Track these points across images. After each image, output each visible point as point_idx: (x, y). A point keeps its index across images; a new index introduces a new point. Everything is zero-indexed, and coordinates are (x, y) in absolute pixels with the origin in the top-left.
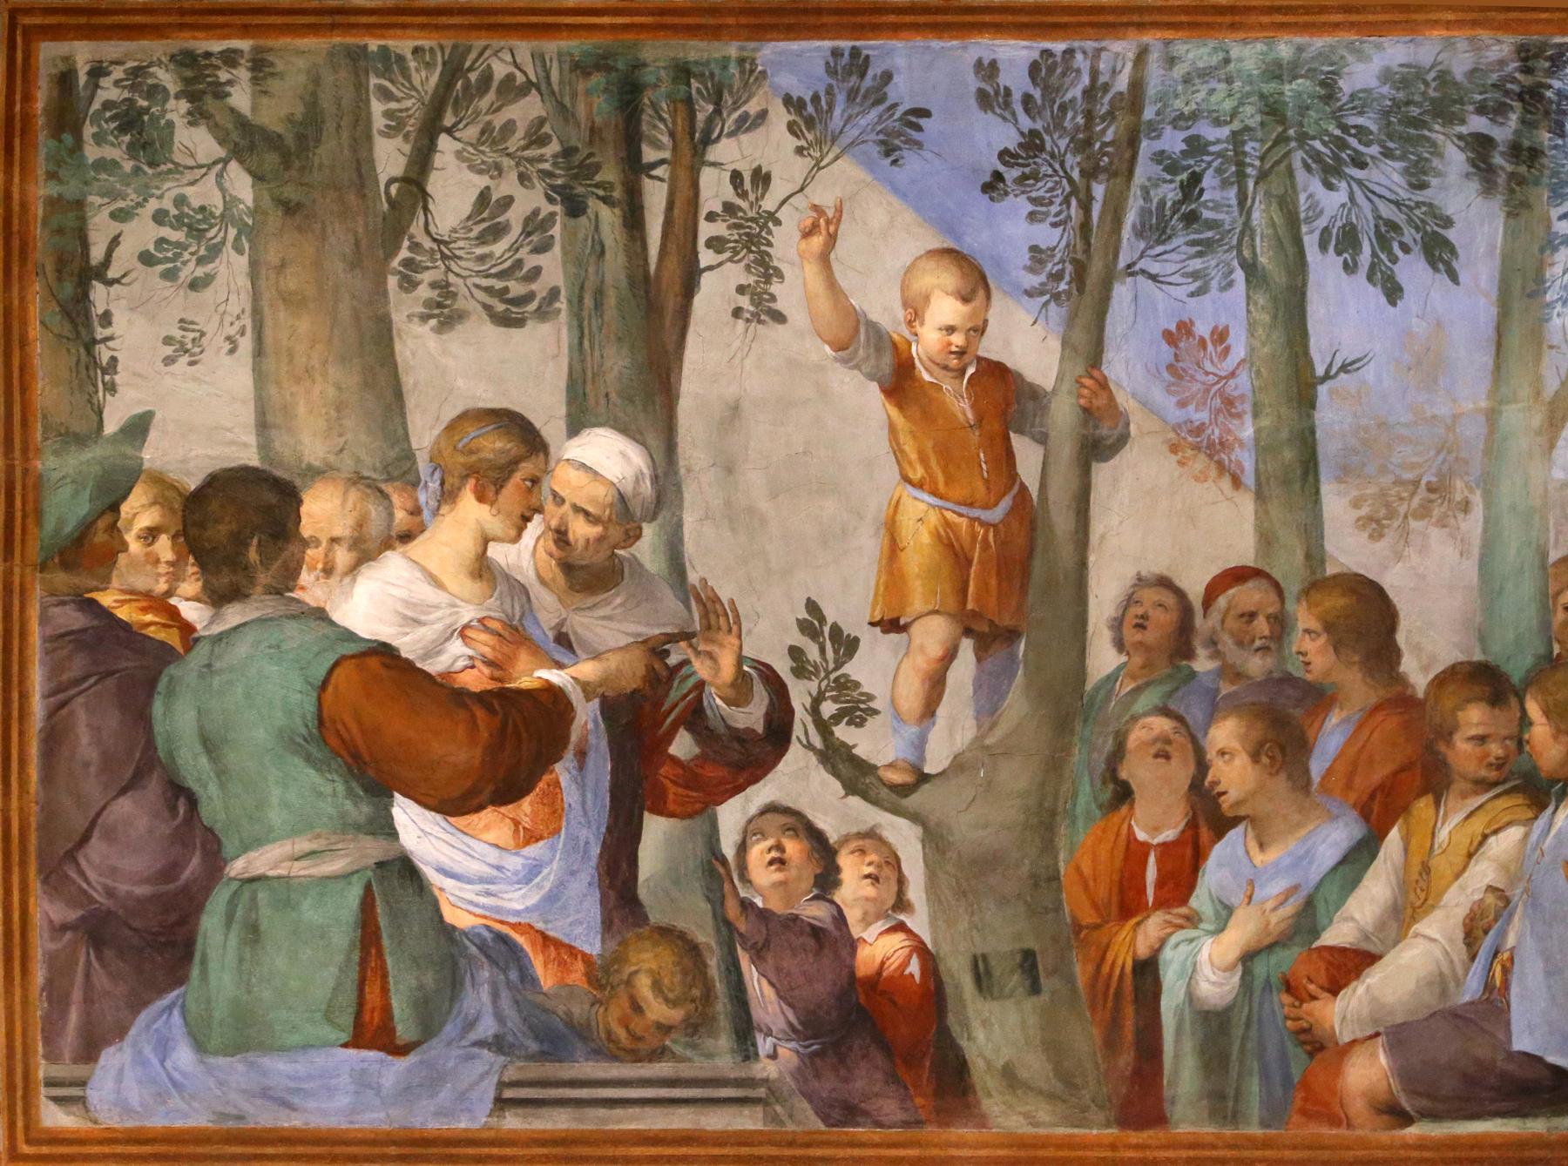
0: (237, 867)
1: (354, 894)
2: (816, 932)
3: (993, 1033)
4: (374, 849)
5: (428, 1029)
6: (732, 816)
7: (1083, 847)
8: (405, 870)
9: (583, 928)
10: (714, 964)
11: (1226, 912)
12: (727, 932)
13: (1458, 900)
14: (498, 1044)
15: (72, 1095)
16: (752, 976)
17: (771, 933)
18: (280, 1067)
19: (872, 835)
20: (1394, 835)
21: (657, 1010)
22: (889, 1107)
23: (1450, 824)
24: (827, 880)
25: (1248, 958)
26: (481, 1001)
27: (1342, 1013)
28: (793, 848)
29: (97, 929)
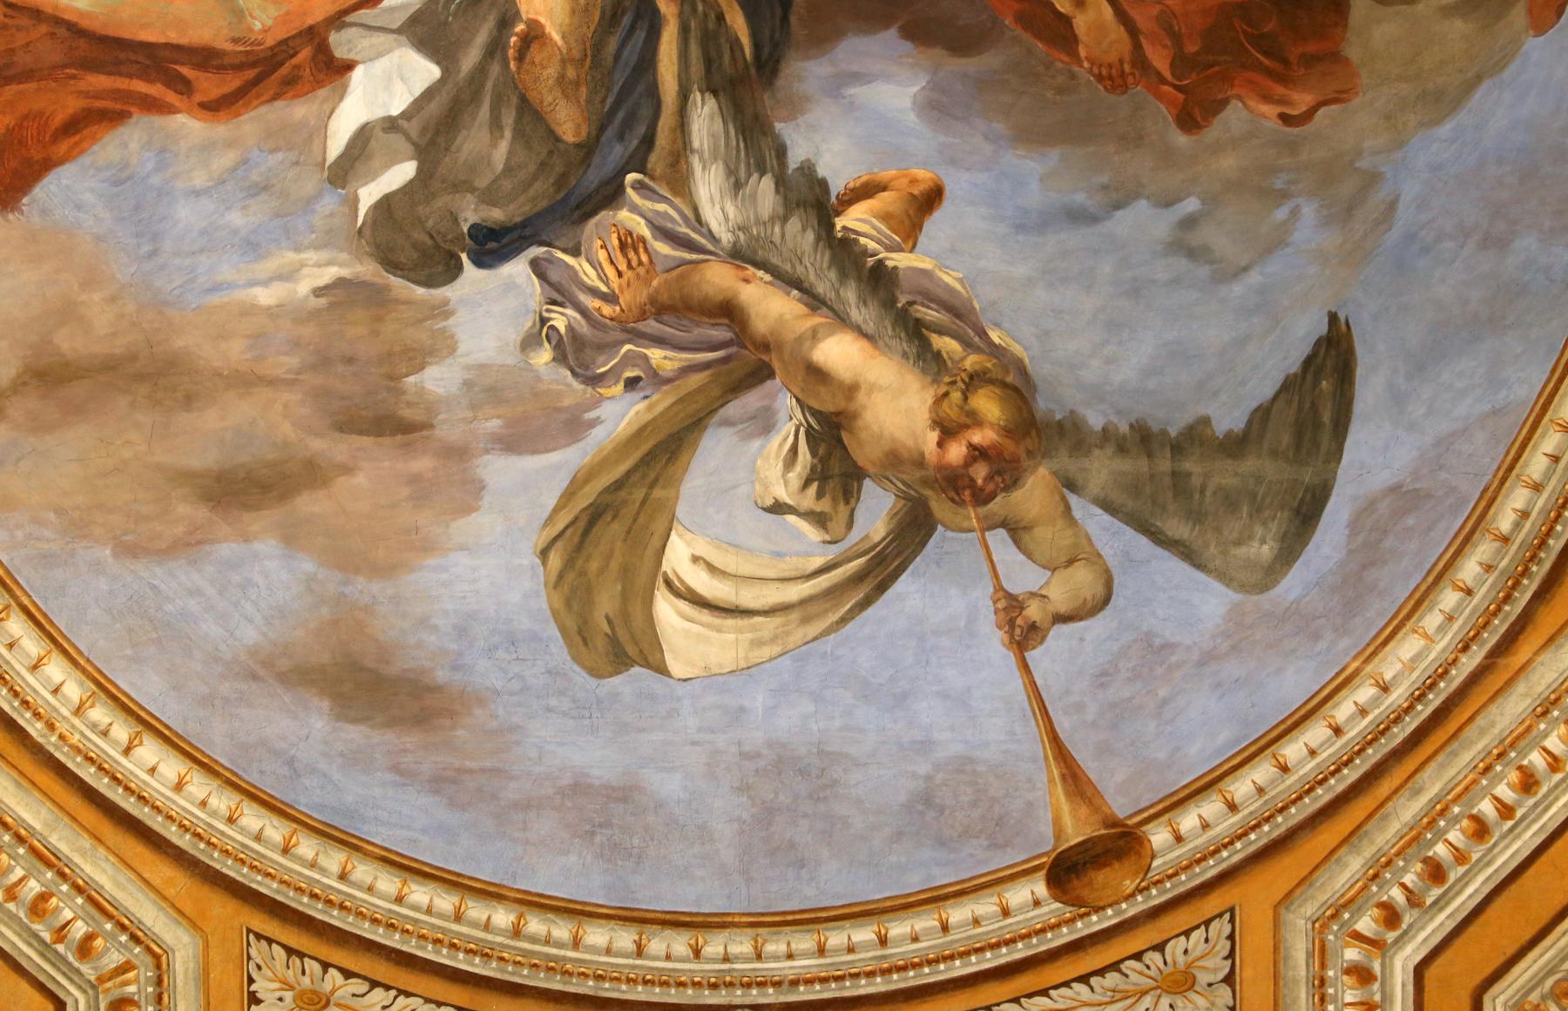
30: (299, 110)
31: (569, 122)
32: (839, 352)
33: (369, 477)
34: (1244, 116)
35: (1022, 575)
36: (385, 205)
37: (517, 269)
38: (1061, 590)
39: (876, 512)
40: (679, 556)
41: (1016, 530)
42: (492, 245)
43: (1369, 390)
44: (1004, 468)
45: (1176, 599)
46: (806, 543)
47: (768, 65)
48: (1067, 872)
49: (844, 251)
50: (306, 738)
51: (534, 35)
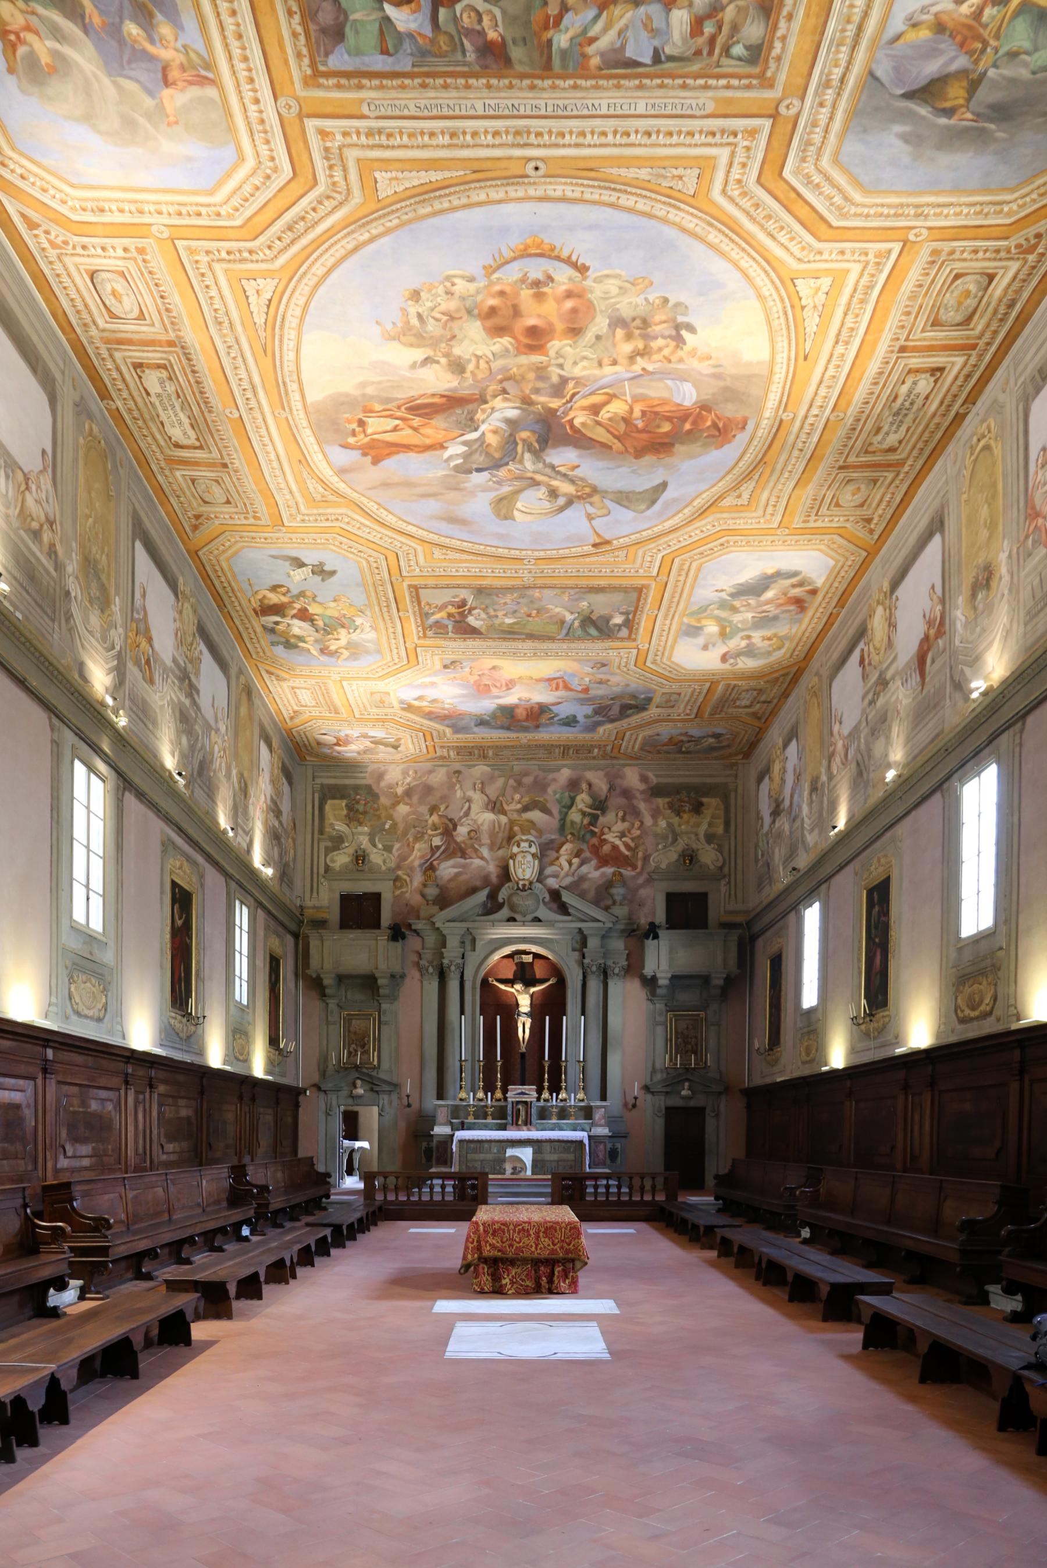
0: (352, 17)
1: (377, 25)
2: (479, 32)
3: (516, 53)
4: (380, 14)
5: (397, 52)
6: (458, 7)
7: (537, 16)
8: (387, 19)
9: (428, 31)
10: (457, 39)
11: (567, 29)
12: (459, 32)
13: (617, 27)
14: (412, 54)
15: (325, 64)
16: (465, 41)
17: (469, 32)
18: (366, 59)
19: (490, 12)
20: (605, 13)
21: (445, 48)
22: (495, 66)
23: (617, 11)
24: (480, 21)
25: (571, 39)
26: (407, 45)
27: (590, 50)
28: (473, 14)
29: (324, 31)
30: (437, 453)
31: (497, 455)
32: (555, 483)
33: (452, 495)
34: (648, 459)
35: (591, 510)
36: (456, 466)
37: (486, 474)
38: (599, 513)
39: (561, 501)
40: (519, 505)
41: (591, 504)
42: (478, 470)
43: (669, 488)
44: (590, 495)
45: (623, 514)
46: (547, 505)
47: (542, 450)
48: (595, 545)
49: (558, 473)
50: (444, 527)
51: (489, 445)
